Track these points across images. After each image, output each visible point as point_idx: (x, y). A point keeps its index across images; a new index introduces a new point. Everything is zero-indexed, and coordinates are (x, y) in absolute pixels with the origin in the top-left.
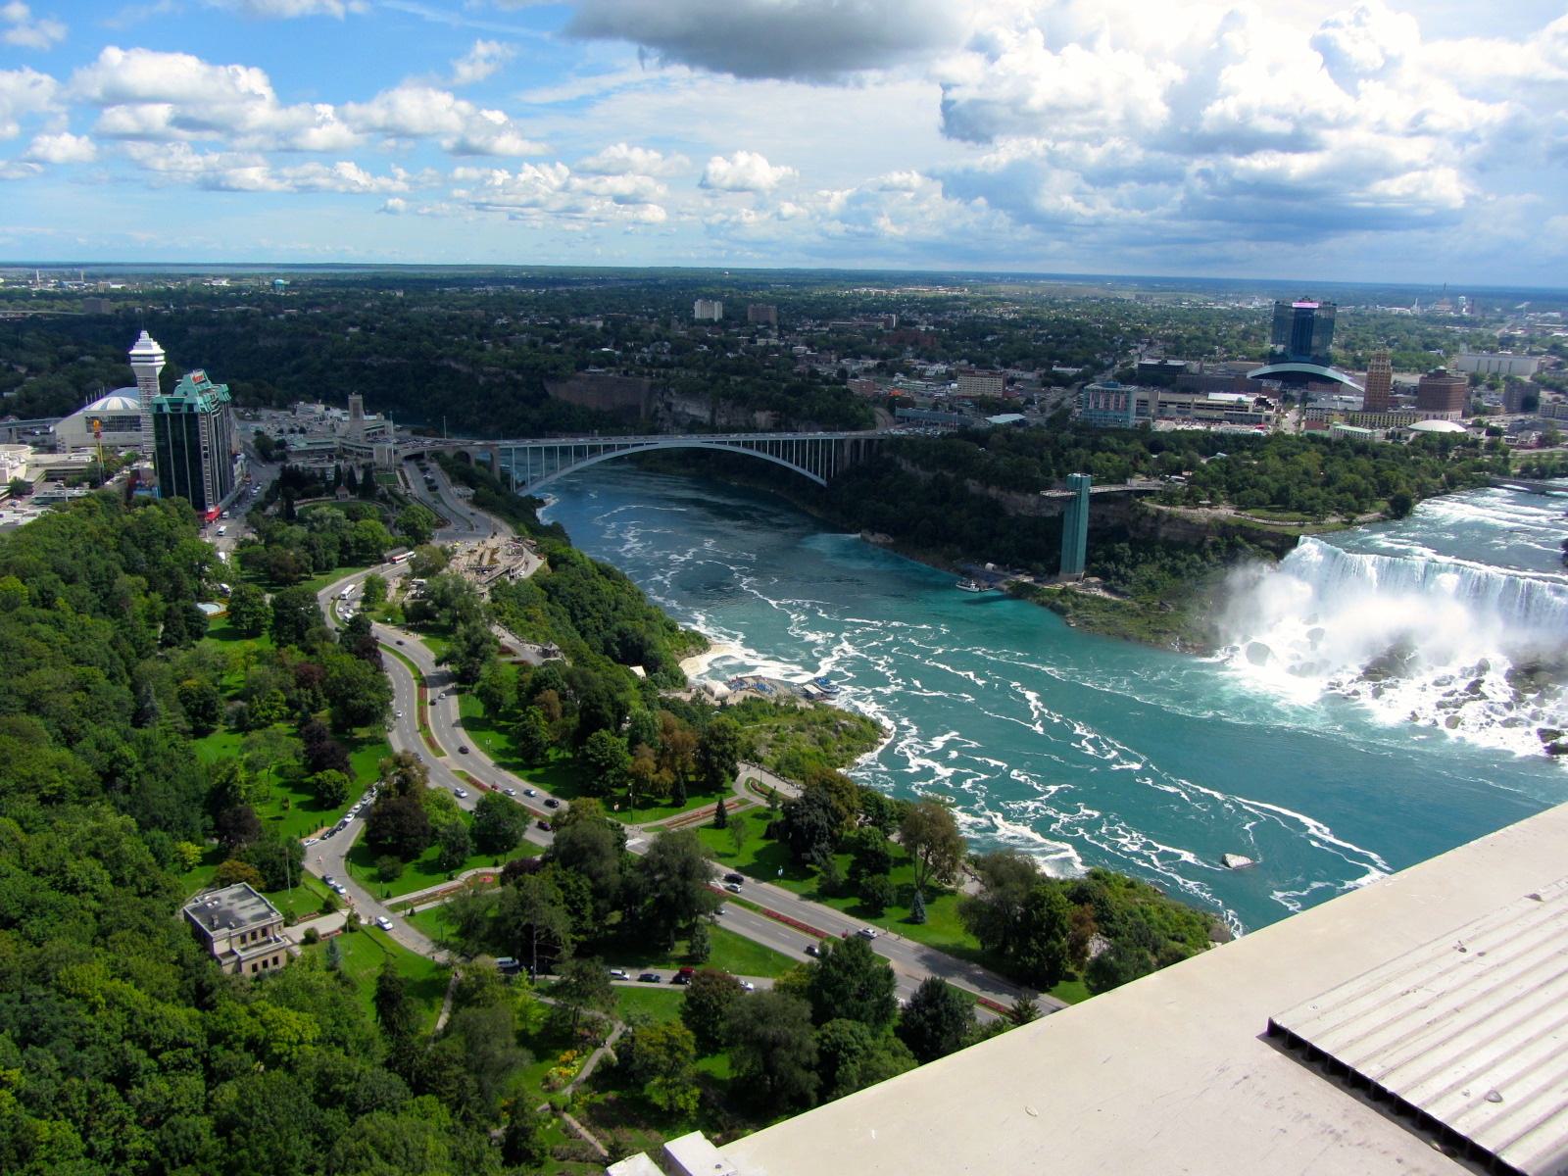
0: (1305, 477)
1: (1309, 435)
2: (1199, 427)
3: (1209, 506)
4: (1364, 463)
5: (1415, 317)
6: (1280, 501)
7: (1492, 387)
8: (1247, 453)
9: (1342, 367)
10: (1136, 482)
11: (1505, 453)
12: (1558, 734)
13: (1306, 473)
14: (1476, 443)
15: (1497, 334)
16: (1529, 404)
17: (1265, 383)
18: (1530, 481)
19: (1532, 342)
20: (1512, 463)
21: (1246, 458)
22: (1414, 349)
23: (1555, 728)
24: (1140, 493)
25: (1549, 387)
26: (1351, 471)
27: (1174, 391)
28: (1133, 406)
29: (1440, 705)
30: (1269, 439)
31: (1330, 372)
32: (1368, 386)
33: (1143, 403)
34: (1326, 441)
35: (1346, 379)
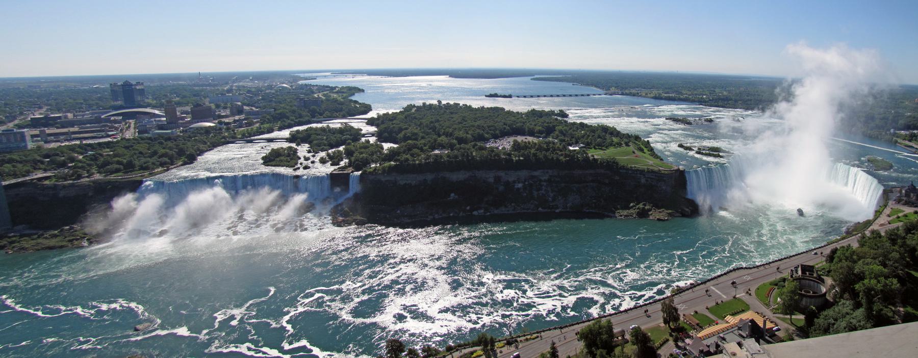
0: (141, 155)
1: (140, 138)
2: (78, 142)
3: (87, 177)
4: (170, 144)
5: (189, 85)
6: (129, 167)
7: (225, 108)
8: (108, 150)
9: (154, 107)
10: (40, 175)
11: (233, 131)
12: (275, 225)
13: (141, 153)
14: (220, 129)
15: (225, 89)
16: (240, 111)
17: (112, 118)
18: (245, 139)
19: (240, 90)
20: (237, 134)
21: (106, 152)
22: (190, 97)
23: (276, 222)
24: (40, 179)
25: (248, 105)
26: (164, 148)
27: (58, 128)
28: (28, 138)
29: (229, 228)
30: (118, 142)
31: (148, 110)
32: (165, 113)
33: (33, 136)
34: (150, 139)
35: (157, 112)
